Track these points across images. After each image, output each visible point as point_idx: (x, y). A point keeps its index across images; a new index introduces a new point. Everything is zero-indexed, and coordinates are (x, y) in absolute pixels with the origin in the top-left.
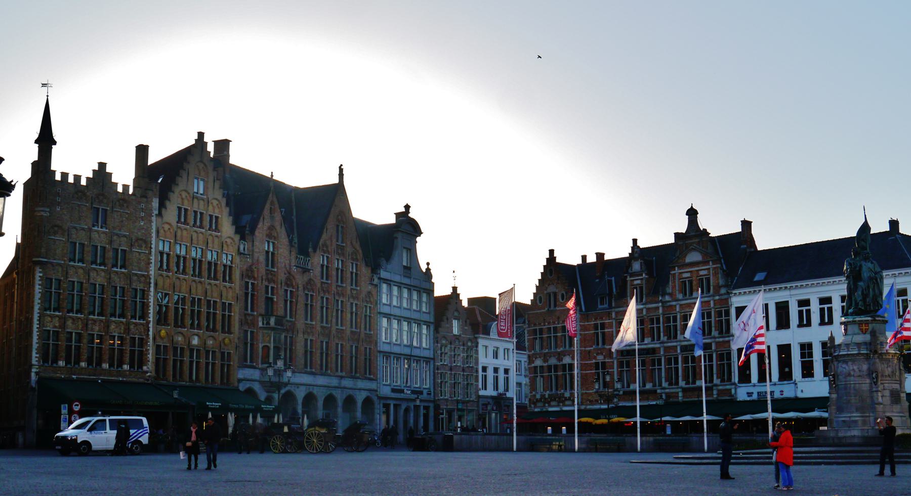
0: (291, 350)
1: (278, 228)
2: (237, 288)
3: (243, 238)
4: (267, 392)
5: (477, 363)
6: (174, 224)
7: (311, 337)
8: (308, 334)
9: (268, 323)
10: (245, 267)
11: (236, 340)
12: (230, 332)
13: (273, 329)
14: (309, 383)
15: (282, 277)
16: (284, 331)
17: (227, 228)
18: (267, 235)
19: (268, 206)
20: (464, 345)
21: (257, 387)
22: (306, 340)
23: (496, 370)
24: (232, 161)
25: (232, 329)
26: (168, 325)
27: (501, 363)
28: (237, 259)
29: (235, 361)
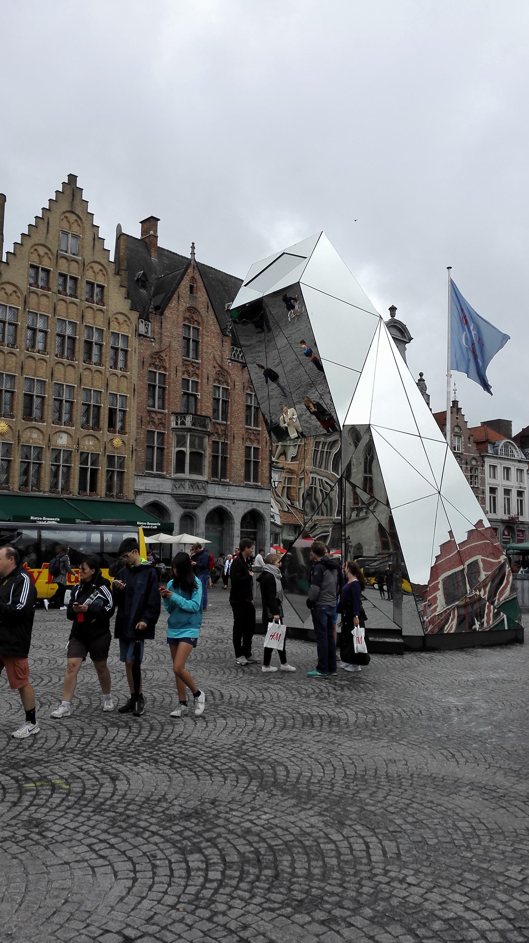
0: (224, 459)
1: (203, 311)
2: (135, 380)
3: (144, 316)
4: (185, 507)
5: (483, 484)
6: (24, 286)
7: (255, 445)
8: (251, 441)
9: (183, 423)
10: (148, 352)
11: (132, 442)
12: (123, 431)
13: (189, 430)
14: (252, 498)
15: (209, 369)
16: (209, 434)
17: (117, 301)
18: (185, 319)
19: (185, 283)
20: (466, 463)
21: (167, 502)
22: (248, 448)
23: (507, 492)
24: (162, 243)
25: (127, 429)
26: (12, 417)
27: (513, 483)
28: (134, 342)
29: (130, 468)
